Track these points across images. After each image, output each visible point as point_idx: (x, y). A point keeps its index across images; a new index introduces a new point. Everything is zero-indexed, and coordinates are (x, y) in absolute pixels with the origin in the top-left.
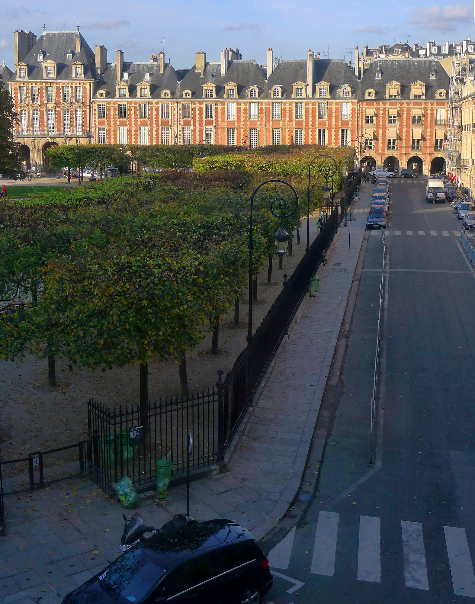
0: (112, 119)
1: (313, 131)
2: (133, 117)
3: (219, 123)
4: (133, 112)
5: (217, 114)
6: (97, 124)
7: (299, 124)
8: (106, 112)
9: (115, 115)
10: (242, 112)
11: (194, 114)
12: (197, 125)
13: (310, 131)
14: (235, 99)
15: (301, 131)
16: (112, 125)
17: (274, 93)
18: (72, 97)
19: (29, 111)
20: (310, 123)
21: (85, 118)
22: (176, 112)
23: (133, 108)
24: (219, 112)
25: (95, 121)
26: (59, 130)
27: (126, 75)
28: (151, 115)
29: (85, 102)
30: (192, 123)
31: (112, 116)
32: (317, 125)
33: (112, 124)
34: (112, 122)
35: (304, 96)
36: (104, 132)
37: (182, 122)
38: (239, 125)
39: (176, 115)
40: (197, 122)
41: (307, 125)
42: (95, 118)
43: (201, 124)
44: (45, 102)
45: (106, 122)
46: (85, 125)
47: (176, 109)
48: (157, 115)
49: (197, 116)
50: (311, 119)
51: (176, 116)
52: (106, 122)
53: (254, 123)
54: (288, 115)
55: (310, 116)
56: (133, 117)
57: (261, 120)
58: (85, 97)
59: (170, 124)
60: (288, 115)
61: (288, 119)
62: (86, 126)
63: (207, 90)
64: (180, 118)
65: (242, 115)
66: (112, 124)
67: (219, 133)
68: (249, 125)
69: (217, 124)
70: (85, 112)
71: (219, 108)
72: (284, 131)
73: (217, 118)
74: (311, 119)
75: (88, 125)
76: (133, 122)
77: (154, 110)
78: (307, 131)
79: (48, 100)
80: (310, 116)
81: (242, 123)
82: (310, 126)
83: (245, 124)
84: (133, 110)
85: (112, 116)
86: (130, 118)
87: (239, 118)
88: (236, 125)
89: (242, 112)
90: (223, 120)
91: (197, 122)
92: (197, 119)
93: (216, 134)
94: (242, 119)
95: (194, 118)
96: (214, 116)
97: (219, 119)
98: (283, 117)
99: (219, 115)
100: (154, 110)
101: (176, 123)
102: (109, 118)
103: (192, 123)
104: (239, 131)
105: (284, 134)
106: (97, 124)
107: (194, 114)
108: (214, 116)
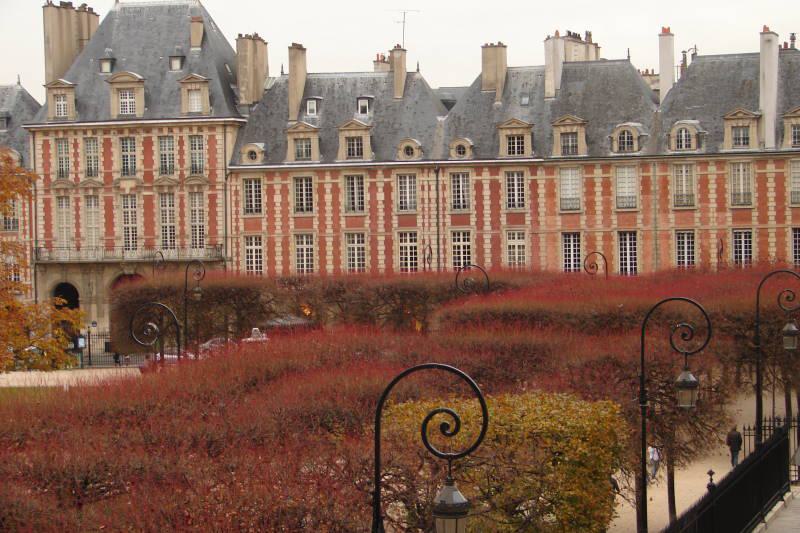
0: (278, 216)
1: (780, 234)
2: (329, 208)
3: (542, 218)
4: (328, 197)
5: (535, 196)
6: (242, 228)
7: (742, 214)
8: (264, 199)
9: (285, 204)
10: (598, 189)
11: (479, 198)
12: (487, 227)
13: (772, 235)
14: (581, 159)
15: (749, 235)
16: (278, 231)
17: (679, 141)
18: (182, 162)
19: (77, 200)
20: (772, 213)
21: (213, 214)
22: (433, 194)
23: (328, 188)
24: (542, 191)
25: (237, 220)
26: (149, 246)
27: (311, 105)
28: (374, 203)
29: (213, 173)
30: (473, 220)
31: (278, 209)
32: (789, 218)
33: (278, 227)
34: (278, 224)
35: (754, 147)
36: (258, 247)
37: (448, 220)
38: (591, 223)
39: (433, 201)
40: (487, 219)
41: (763, 219)
42: (237, 213)
43: (495, 224)
44: (116, 176)
45: (264, 224)
46: (213, 231)
47: (433, 188)
48: (388, 201)
49: (487, 203)
50: (772, 204)
51: (433, 205)
52: (264, 224)
53: (627, 213)
54: (713, 196)
55: (771, 195)
56: (329, 208)
57: (646, 209)
58: (212, 161)
59: (419, 224)
60: (713, 196)
61: (713, 205)
62: (216, 232)
63: (510, 138)
64: (444, 209)
65: (599, 198)
66: (278, 227)
67: (543, 243)
68: (615, 222)
69: (536, 222)
70: (213, 198)
71: (541, 183)
72: (706, 234)
73: (535, 206)
74: (772, 204)
75: (220, 232)
76: (329, 222)
77: (380, 190)
78: (764, 234)
79: (125, 171)
80: (771, 195)
81: (599, 217)
82: (772, 222)
83: (607, 222)
84: (328, 191)
85: (278, 209)
86: (322, 211)
87: (590, 204)
88: (583, 222)
89: (598, 189)
90: (551, 212)
91: (487, 219)
92: (487, 211)
93: (535, 248)
94: (599, 208)
95: (480, 207)
96: (528, 202)
97: (542, 209)
98: (701, 201)
99: (542, 200)
100: (380, 190)
101: (434, 221)
102: (271, 213)
103: (473, 220)
104: (591, 240)
105: (705, 244)
106: (242, 228)
107: (479, 198)
108: (528, 202)
